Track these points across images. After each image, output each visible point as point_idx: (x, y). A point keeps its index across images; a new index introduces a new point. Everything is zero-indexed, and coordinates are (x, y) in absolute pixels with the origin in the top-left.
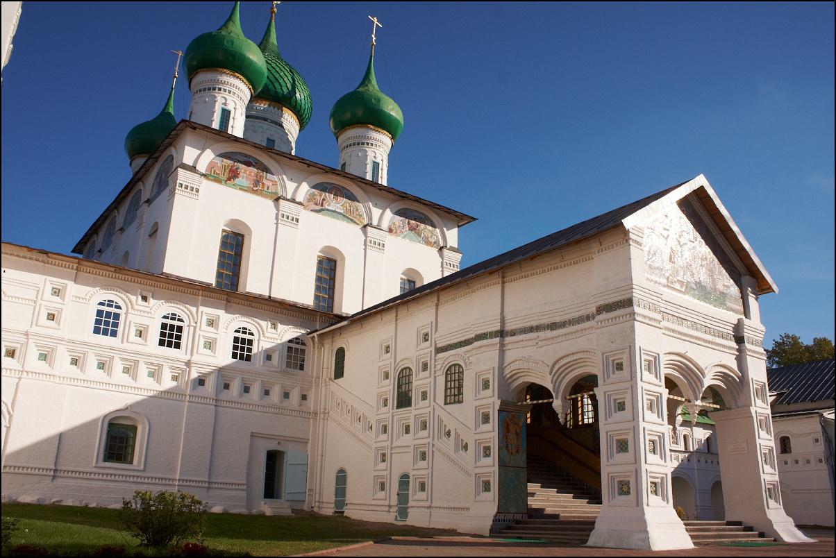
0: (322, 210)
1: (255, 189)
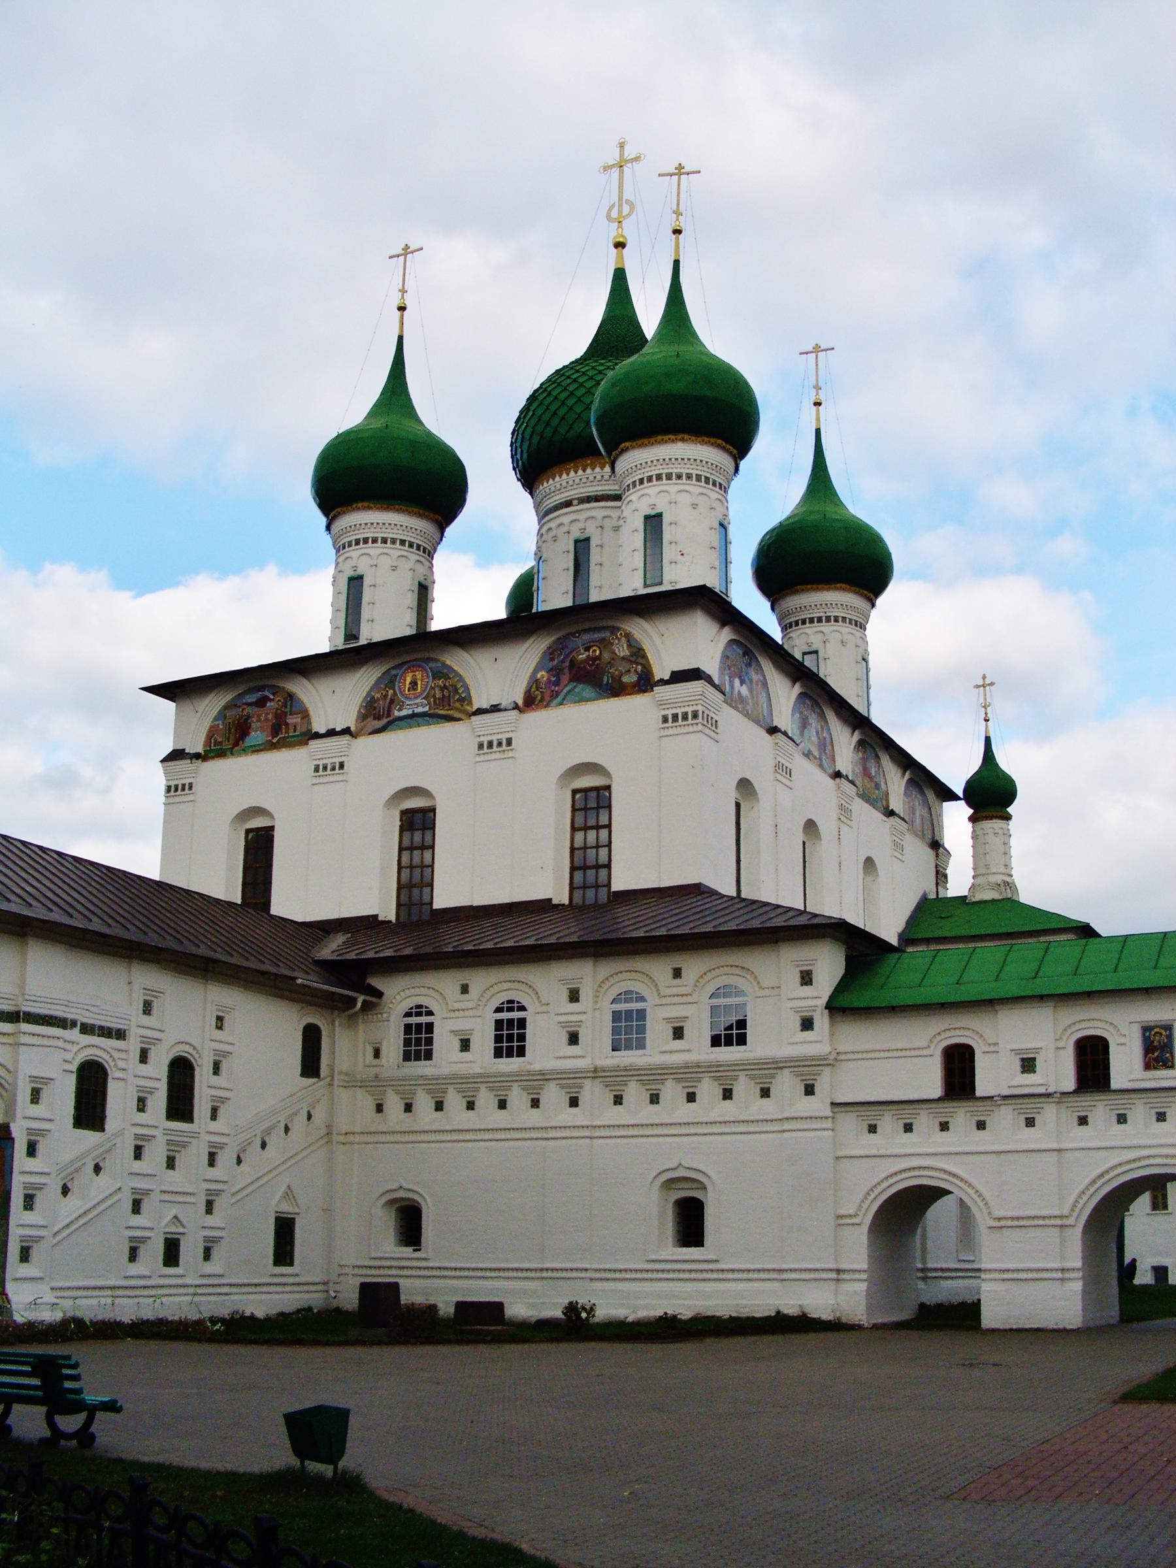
1: (275, 740)
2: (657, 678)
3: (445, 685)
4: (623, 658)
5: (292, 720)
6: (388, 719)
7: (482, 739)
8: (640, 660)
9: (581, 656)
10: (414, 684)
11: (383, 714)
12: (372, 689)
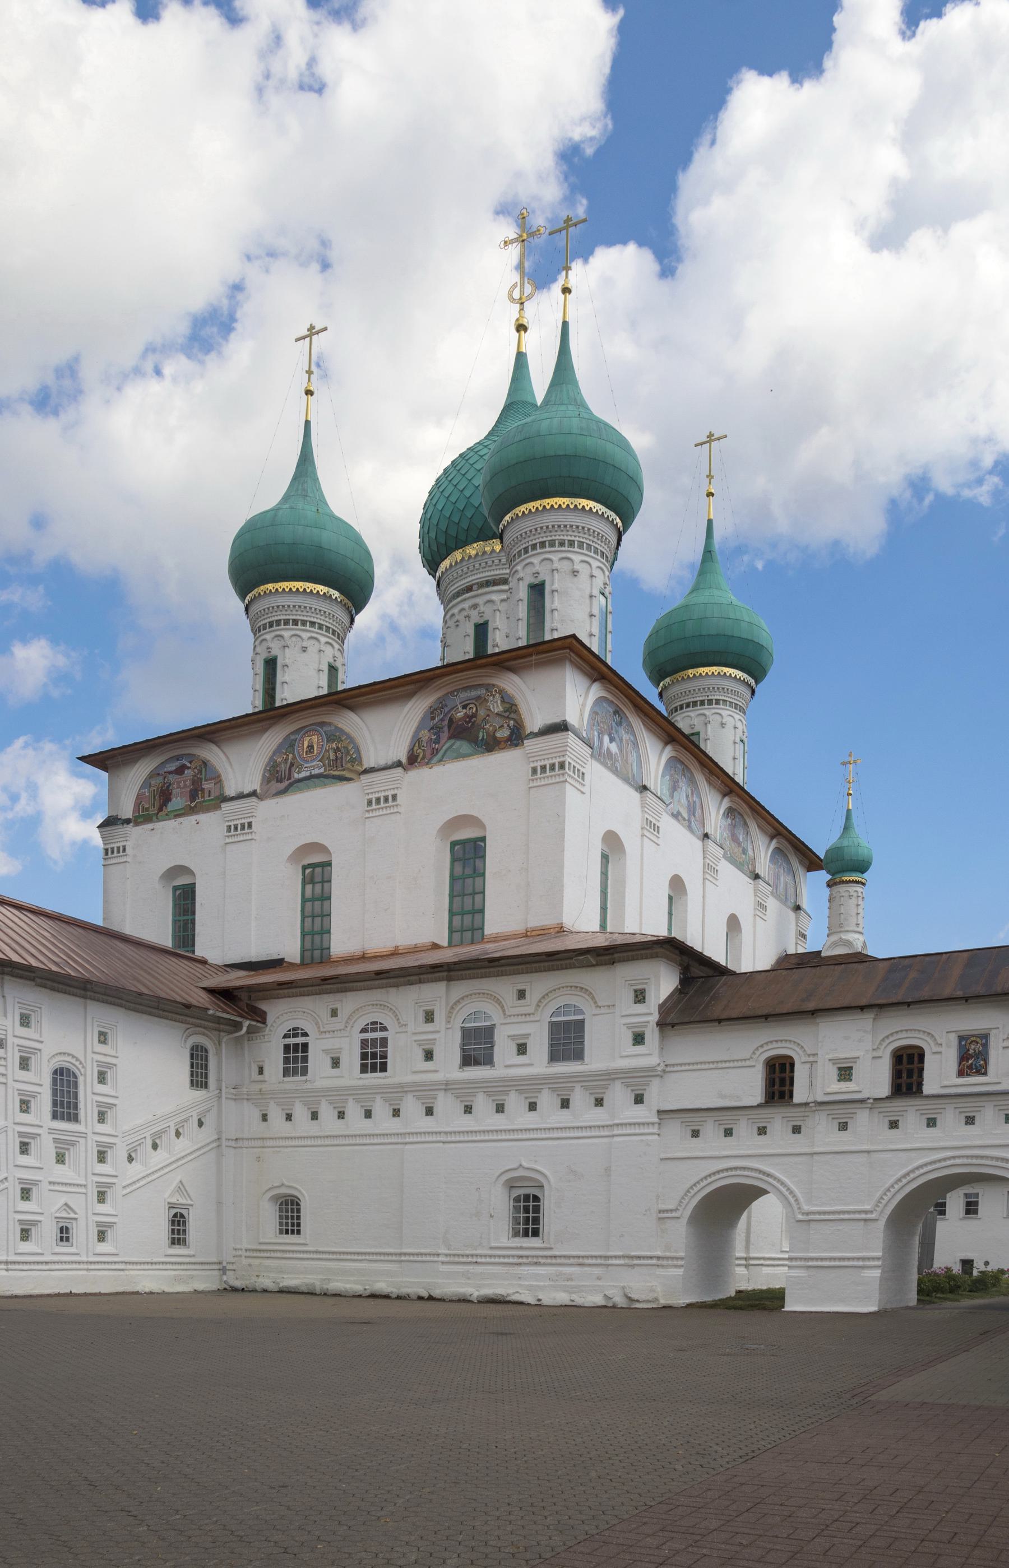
0: (291, 785)
1: (193, 805)
2: (528, 731)
3: (338, 747)
4: (497, 714)
5: (206, 786)
6: (290, 781)
7: (370, 796)
8: (512, 716)
9: (459, 714)
10: (311, 747)
11: (285, 776)
12: (274, 753)
